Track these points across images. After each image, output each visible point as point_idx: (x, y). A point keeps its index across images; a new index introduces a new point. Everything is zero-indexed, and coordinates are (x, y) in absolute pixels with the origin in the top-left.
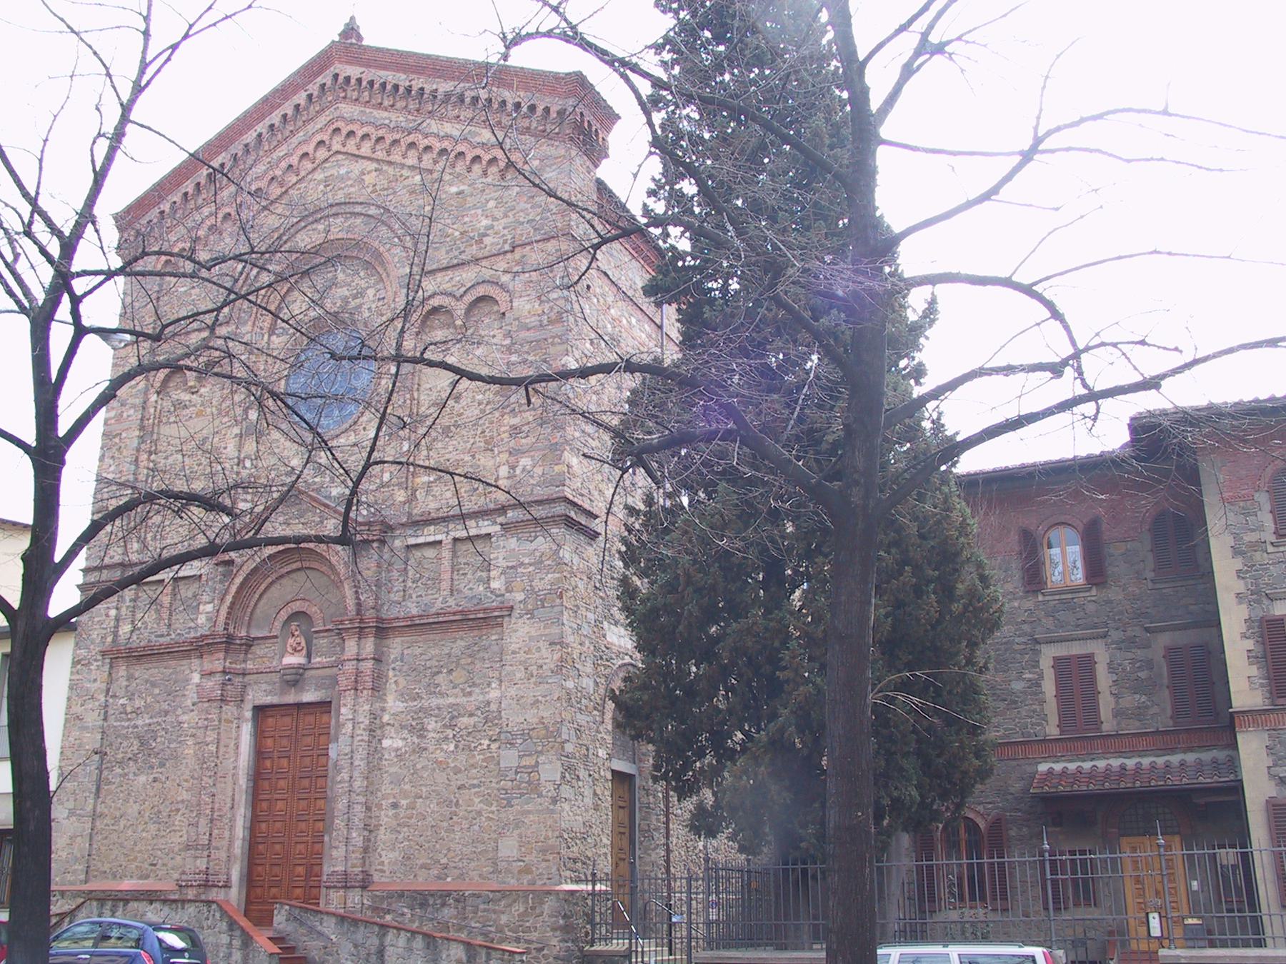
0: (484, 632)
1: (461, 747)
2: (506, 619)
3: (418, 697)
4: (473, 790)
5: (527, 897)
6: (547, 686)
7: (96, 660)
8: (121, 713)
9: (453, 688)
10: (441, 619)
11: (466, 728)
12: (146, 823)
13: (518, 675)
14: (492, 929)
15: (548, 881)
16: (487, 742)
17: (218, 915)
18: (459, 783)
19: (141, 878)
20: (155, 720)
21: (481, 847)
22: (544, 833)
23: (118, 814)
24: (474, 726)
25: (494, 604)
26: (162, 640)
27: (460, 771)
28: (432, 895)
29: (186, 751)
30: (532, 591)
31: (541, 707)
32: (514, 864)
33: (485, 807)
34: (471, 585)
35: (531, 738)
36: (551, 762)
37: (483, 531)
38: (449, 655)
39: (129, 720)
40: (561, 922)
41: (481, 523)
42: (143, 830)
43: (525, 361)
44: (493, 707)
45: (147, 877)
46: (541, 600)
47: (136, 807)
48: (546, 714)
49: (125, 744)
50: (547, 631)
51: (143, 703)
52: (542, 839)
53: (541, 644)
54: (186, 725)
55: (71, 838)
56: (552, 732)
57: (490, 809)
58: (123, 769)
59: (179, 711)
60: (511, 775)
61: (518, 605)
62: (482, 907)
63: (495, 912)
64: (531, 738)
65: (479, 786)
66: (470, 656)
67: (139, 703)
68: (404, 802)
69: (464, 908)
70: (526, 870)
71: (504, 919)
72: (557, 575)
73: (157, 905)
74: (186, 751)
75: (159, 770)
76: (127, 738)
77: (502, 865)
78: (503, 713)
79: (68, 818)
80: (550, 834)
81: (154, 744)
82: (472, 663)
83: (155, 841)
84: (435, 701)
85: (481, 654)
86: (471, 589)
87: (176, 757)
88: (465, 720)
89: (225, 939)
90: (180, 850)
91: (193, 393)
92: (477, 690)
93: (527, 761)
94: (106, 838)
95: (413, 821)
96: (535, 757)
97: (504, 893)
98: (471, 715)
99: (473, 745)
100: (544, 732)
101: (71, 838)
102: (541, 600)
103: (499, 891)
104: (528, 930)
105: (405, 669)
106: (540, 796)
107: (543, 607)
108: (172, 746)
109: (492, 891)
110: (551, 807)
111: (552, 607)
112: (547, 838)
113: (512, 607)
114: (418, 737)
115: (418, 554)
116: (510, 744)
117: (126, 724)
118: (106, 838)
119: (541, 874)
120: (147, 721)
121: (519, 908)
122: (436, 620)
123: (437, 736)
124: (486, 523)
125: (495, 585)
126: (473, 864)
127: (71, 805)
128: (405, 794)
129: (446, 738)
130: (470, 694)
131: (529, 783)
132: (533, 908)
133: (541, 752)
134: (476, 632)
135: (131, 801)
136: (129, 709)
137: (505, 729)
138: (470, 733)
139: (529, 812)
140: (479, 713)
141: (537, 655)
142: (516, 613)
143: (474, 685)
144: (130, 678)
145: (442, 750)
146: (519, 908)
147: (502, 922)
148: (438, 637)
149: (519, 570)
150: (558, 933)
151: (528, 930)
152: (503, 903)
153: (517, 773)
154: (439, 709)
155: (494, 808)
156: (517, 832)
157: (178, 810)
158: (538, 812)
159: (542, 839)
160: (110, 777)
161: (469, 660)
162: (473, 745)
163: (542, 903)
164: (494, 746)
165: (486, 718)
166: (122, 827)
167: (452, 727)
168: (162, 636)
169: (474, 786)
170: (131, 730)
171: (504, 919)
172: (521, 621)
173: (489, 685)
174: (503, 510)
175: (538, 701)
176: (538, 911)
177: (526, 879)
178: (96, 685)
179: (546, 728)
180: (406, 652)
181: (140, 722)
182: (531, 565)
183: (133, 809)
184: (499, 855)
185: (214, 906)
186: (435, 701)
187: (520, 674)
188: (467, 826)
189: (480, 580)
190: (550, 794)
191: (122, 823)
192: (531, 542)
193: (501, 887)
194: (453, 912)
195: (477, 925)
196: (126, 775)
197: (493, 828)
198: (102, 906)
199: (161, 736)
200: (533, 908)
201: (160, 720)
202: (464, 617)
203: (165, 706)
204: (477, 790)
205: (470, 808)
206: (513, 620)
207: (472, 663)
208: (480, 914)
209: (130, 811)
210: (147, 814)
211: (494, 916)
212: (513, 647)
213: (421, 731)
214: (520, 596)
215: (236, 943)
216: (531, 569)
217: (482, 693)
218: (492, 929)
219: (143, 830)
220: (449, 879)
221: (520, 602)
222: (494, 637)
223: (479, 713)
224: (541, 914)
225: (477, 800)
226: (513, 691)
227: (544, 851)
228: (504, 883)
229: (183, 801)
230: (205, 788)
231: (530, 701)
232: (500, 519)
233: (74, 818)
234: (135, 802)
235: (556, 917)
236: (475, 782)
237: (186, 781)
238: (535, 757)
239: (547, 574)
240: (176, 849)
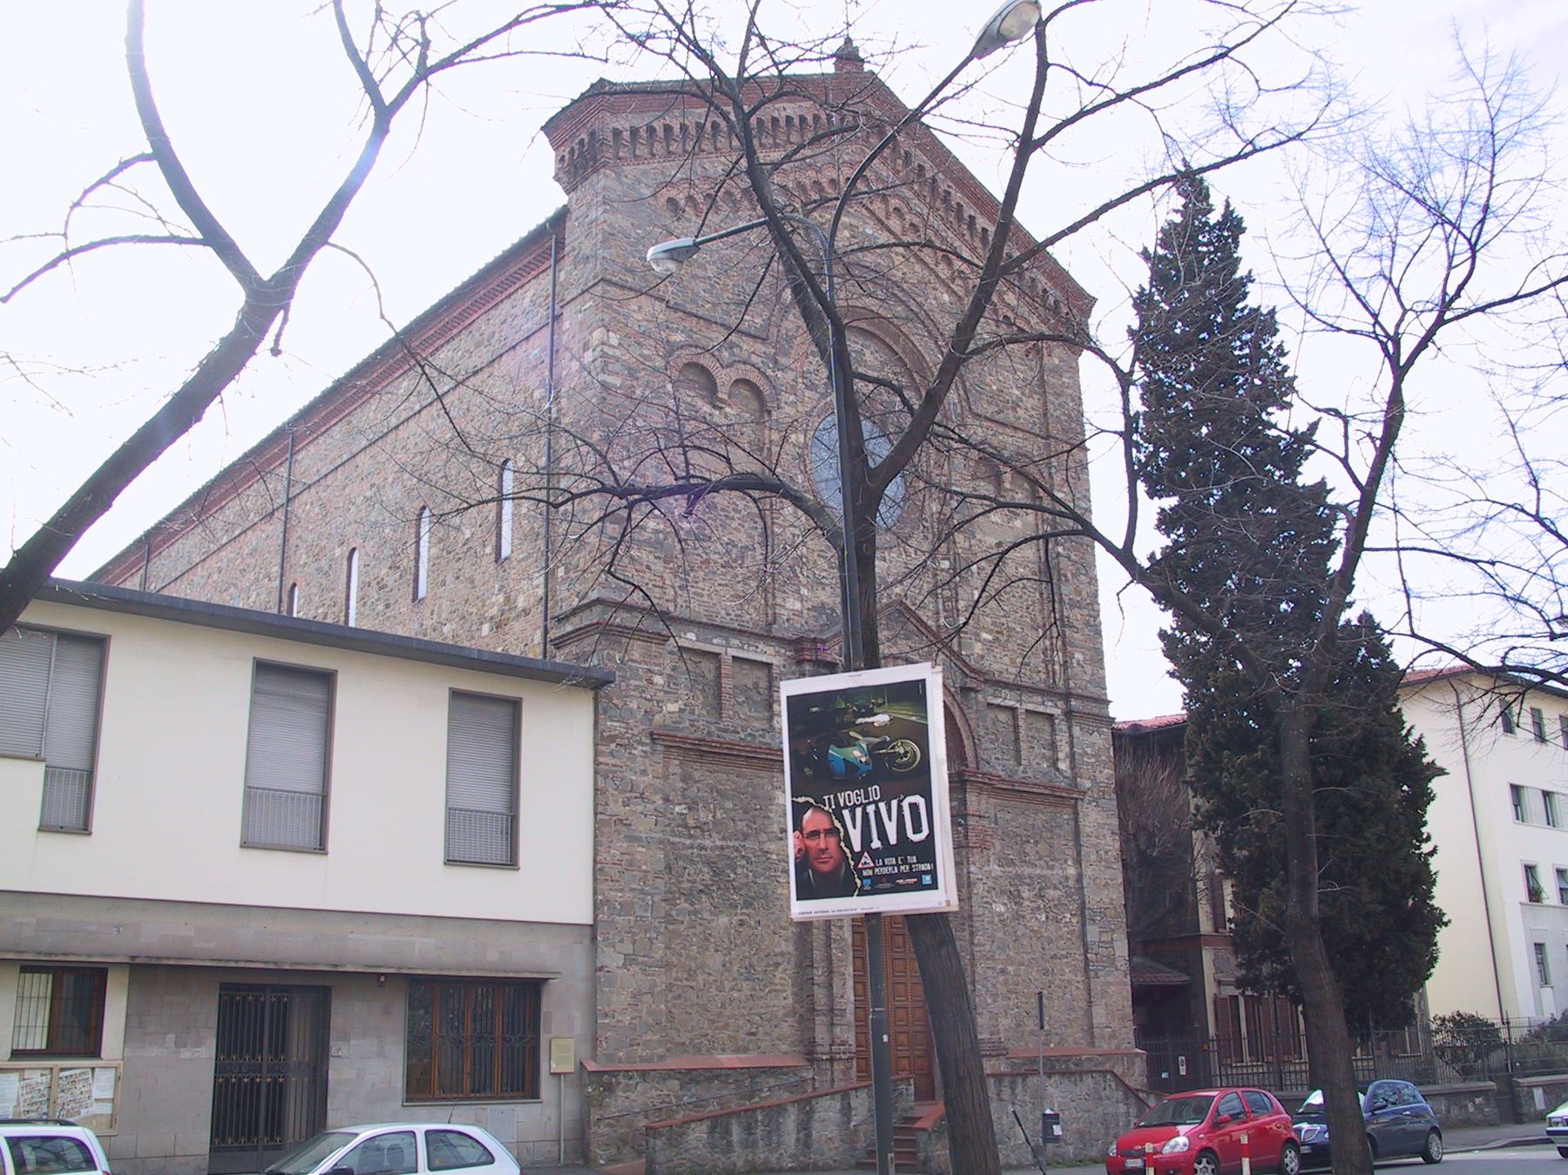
0: (1059, 809)
2: (1080, 802)
3: (1012, 863)
5: (1123, 1059)
7: (640, 743)
8: (679, 826)
9: (1040, 859)
10: (1035, 790)
11: (1053, 900)
12: (734, 979)
17: (1113, 1084)
18: (1052, 953)
19: (737, 1050)
20: (731, 844)
22: (1121, 1003)
23: (693, 965)
26: (729, 737)
28: (1057, 1061)
29: (779, 891)
34: (1037, 761)
37: (1049, 711)
38: (1033, 825)
39: (691, 837)
42: (732, 989)
43: (1069, 558)
45: (746, 1050)
47: (719, 957)
48: (1114, 897)
49: (691, 869)
51: (710, 818)
53: (1105, 832)
54: (774, 857)
55: (634, 996)
58: (692, 904)
59: (763, 837)
65: (1067, 957)
67: (705, 816)
68: (1010, 968)
70: (1113, 1036)
73: (1056, 1078)
74: (779, 891)
75: (747, 911)
76: (692, 862)
77: (1097, 1031)
79: (624, 966)
81: (732, 876)
82: (1052, 838)
83: (751, 1003)
84: (1027, 870)
87: (766, 896)
88: (1051, 892)
89: (1122, 1108)
90: (785, 1015)
91: (714, 407)
93: (1105, 938)
94: (679, 997)
95: (1020, 987)
98: (1055, 888)
101: (634, 996)
105: (1000, 832)
106: (1117, 969)
108: (758, 881)
114: (1016, 903)
115: (991, 714)
117: (688, 842)
118: (679, 997)
120: (719, 843)
122: (1031, 790)
123: (1033, 905)
124: (1050, 704)
127: (628, 947)
128: (1010, 961)
129: (1039, 908)
133: (1113, 931)
135: (711, 947)
136: (691, 823)
139: (1111, 983)
144: (685, 778)
145: (1037, 919)
148: (1024, 805)
154: (1030, 877)
156: (1104, 1001)
157: (777, 965)
159: (1120, 1007)
160: (674, 913)
166: (702, 983)
167: (1042, 897)
168: (726, 731)
170: (695, 851)
173: (1066, 861)
176: (1131, 1072)
178: (646, 779)
180: (999, 815)
181: (707, 843)
182: (1093, 756)
183: (715, 961)
185: (1109, 1076)
186: (1027, 870)
187: (1093, 857)
189: (1044, 756)
191: (701, 978)
196: (696, 912)
198: (1000, 1083)
199: (743, 867)
201: (737, 844)
203: (741, 826)
206: (1085, 806)
207: (1052, 838)
209: (710, 962)
210: (736, 968)
212: (1088, 830)
213: (1016, 898)
215: (1133, 1111)
219: (732, 989)
220: (1052, 1045)
222: (1066, 817)
225: (1067, 970)
227: (1123, 1018)
229: (782, 954)
230: (835, 940)
232: (1059, 703)
233: (636, 968)
234: (717, 951)
236: (1064, 952)
237: (784, 928)
240: (780, 1014)
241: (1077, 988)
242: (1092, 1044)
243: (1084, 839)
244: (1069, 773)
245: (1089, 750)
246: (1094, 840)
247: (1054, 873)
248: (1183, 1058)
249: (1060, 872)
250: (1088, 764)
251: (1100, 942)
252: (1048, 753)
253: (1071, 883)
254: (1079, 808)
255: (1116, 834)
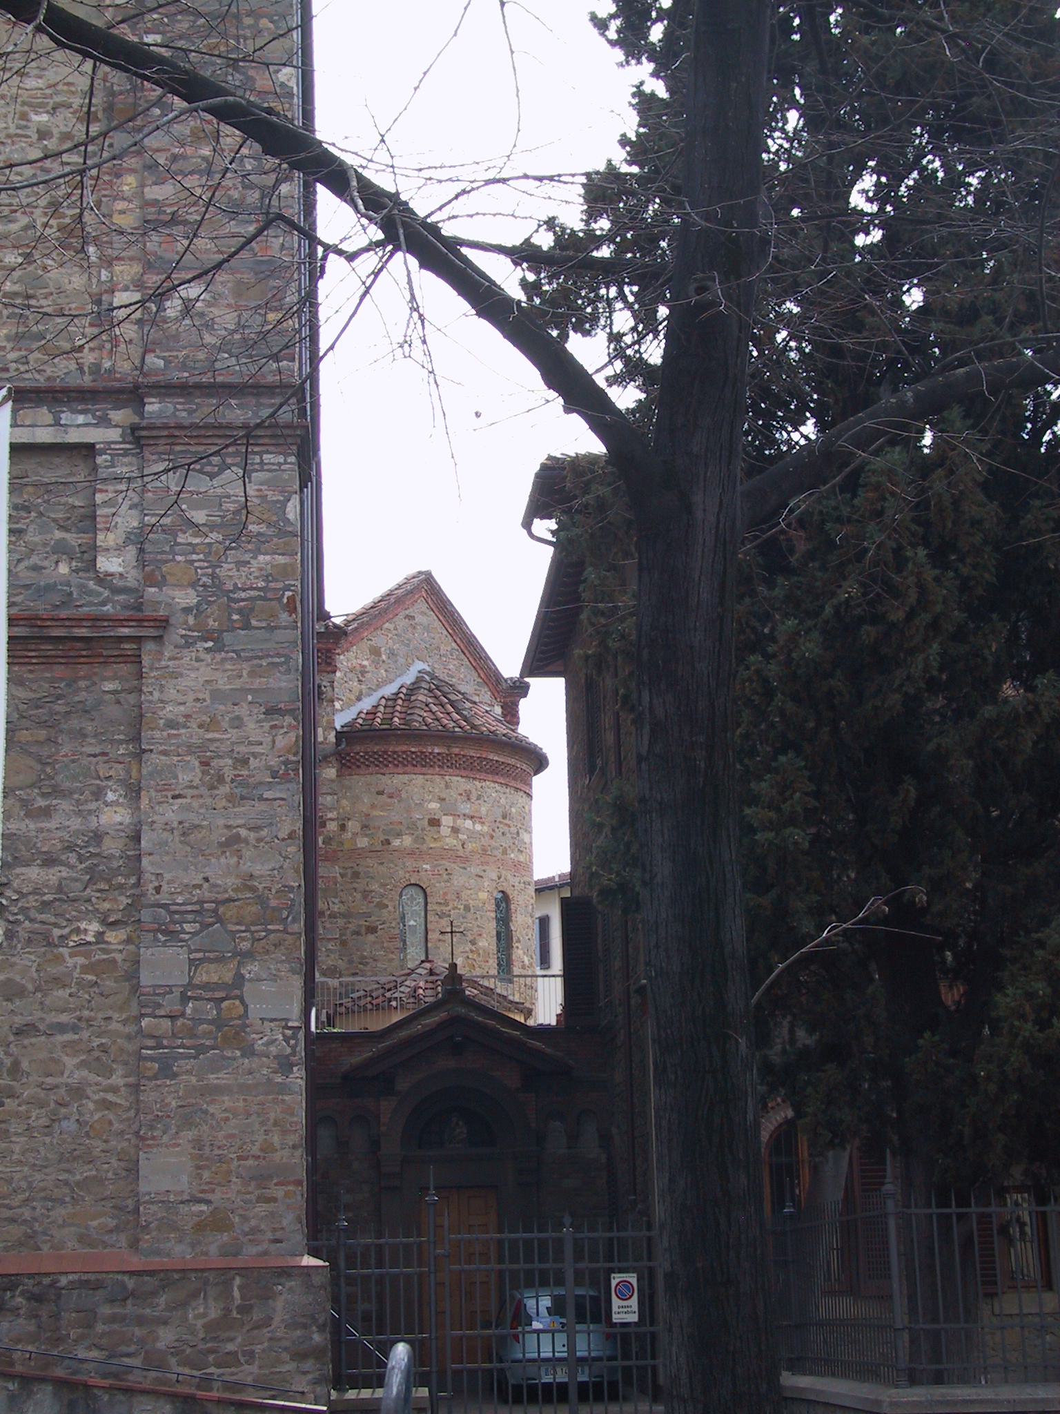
0: (83, 671)
1: (23, 935)
2: (150, 646)
4: (60, 1038)
5: (227, 1284)
6: (262, 806)
11: (36, 892)
13: (184, 777)
14: (136, 1362)
15: (274, 1247)
16: (95, 927)
18: (19, 1020)
21: (83, 1172)
22: (260, 1138)
24: (60, 889)
25: (108, 608)
27: (21, 992)
30: (214, 589)
31: (247, 853)
32: (184, 1209)
33: (93, 1078)
34: (35, 559)
35: (220, 920)
36: (274, 978)
37: (74, 437)
40: (317, 1338)
41: (65, 418)
44: (112, 846)
46: (240, 612)
48: (259, 869)
50: (258, 683)
52: (255, 1150)
56: (277, 910)
57: (105, 1082)
60: (170, 1004)
61: (177, 619)
62: (106, 1310)
63: (141, 1321)
64: (220, 920)
65: (75, 1029)
66: (42, 724)
69: (56, 1316)
70: (218, 1222)
71: (166, 1337)
72: (281, 560)
77: (150, 1212)
78: (145, 861)
80: (276, 1139)
85: (75, 723)
86: (36, 568)
88: (34, 873)
92: (65, 805)
96: (233, 965)
97: (166, 1278)
98: (49, 861)
99: (57, 932)
100: (254, 909)
102: (240, 612)
103: (151, 1273)
104: (230, 1360)
106: (249, 1052)
107: (247, 626)
109: (132, 1273)
110: (279, 1079)
111: (271, 629)
112: (268, 1148)
113: (163, 623)
116: (164, 933)
119: (255, 1230)
121: (206, 1310)
124: (81, 419)
125: (109, 564)
126: (60, 1212)
130: (47, 812)
131: (219, 1023)
132: (245, 1309)
133: (249, 955)
134: (59, 671)
137: (152, 898)
138: (44, 903)
139: (216, 1091)
140: (73, 858)
141: (233, 734)
142: (177, 634)
143: (56, 792)
146: (206, 1310)
147: (160, 1345)
149: (181, 539)
150: (309, 1364)
151: (230, 1360)
152: (162, 1300)
153: (185, 999)
155: (117, 1079)
156: (190, 1134)
158: (244, 1089)
159: (255, 1150)
161: (43, 734)
162: (57, 932)
163: (267, 1296)
164: (112, 937)
165: (90, 870)
169: (62, 1028)
171: (166, 1337)
172: (188, 656)
173: (98, 794)
174: (133, 395)
175: (237, 839)
176: (257, 1315)
177: (214, 1244)
179: (261, 900)
182: (213, 527)
184: (143, 1187)
187: (189, 774)
188: (44, 1121)
189: (61, 550)
190: (273, 1050)
192: (212, 476)
193: (155, 1262)
194: (24, 1325)
195: (94, 1354)
197: (117, 1126)
200: (245, 1309)
202: (36, 632)
204: (69, 1037)
205: (49, 1080)
208: (100, 1328)
211: (138, 1332)
212: (170, 711)
214: (186, 598)
216: (215, 536)
217: (79, 813)
218: (136, 1362)
221: (187, 610)
222: (109, 686)
223: (73, 858)
224: (267, 1321)
225: (70, 1062)
226: (170, 813)
227: (261, 1179)
228: (158, 1252)
231: (220, 835)
232: (117, 416)
235: (305, 1326)
236: (64, 1018)
238: (233, 965)
239: (258, 552)
241: (106, 1105)
242: (134, 1244)
243: (154, 736)
244: (133, 577)
245: (199, 517)
246: (194, 734)
247: (52, 825)
248: (633, 1279)
249: (75, 823)
250: (193, 548)
251: (191, 985)
252: (73, 539)
253: (112, 846)
254: (146, 660)
255: (282, 713)
